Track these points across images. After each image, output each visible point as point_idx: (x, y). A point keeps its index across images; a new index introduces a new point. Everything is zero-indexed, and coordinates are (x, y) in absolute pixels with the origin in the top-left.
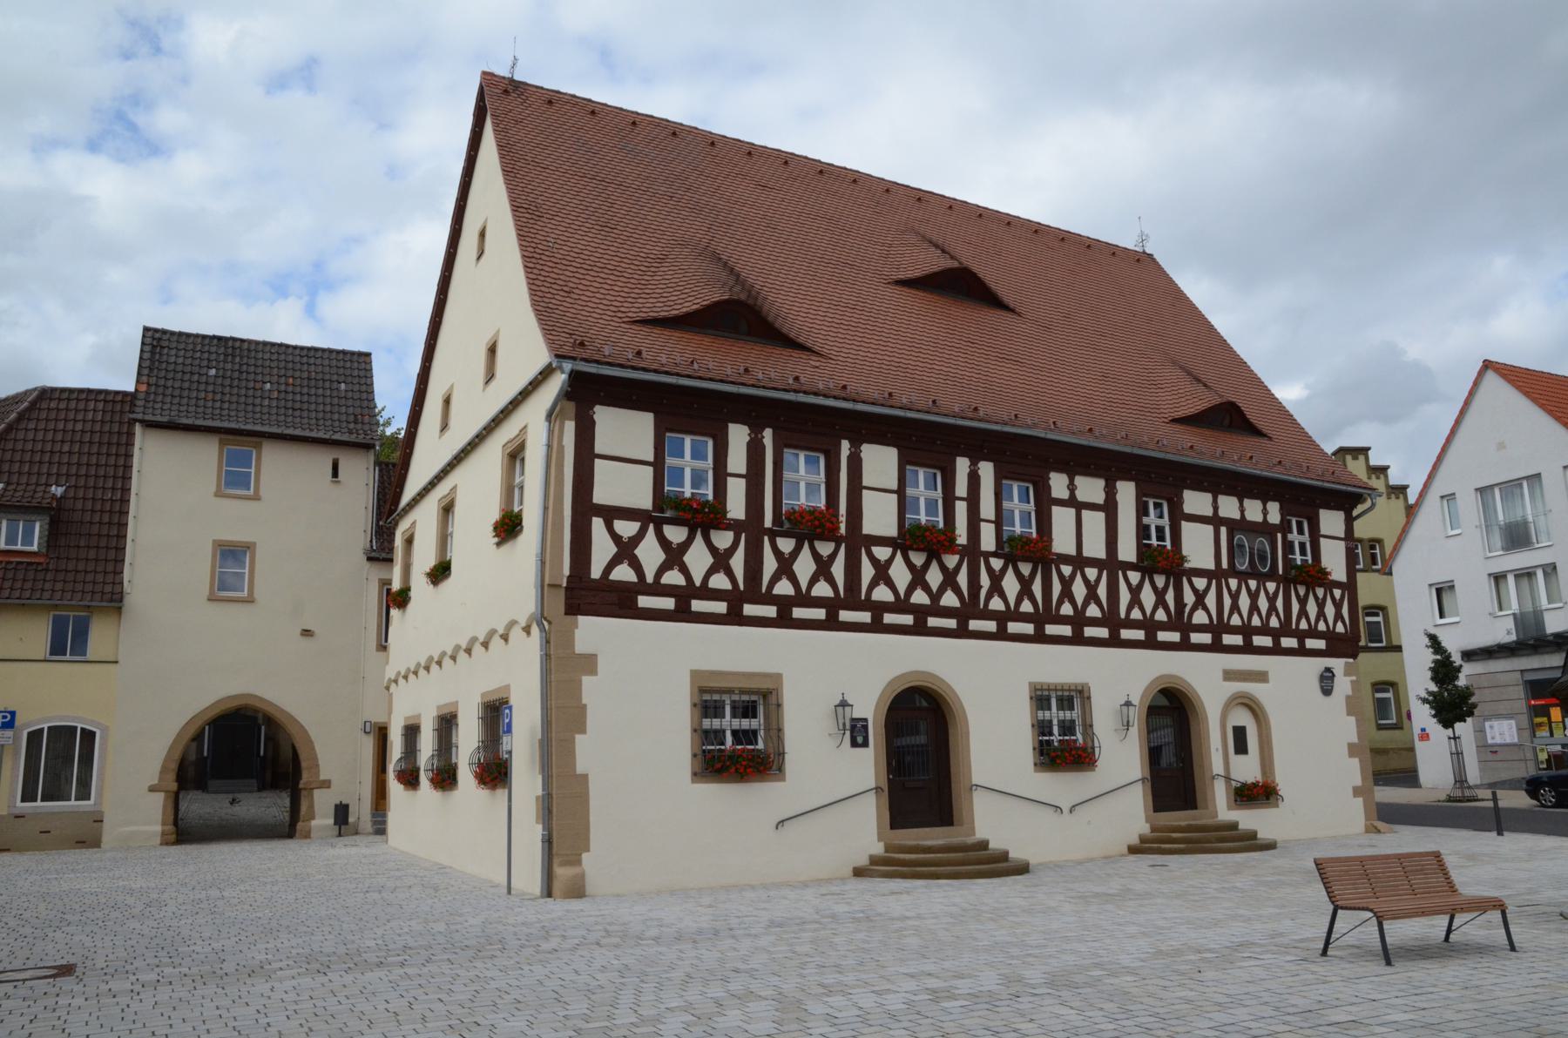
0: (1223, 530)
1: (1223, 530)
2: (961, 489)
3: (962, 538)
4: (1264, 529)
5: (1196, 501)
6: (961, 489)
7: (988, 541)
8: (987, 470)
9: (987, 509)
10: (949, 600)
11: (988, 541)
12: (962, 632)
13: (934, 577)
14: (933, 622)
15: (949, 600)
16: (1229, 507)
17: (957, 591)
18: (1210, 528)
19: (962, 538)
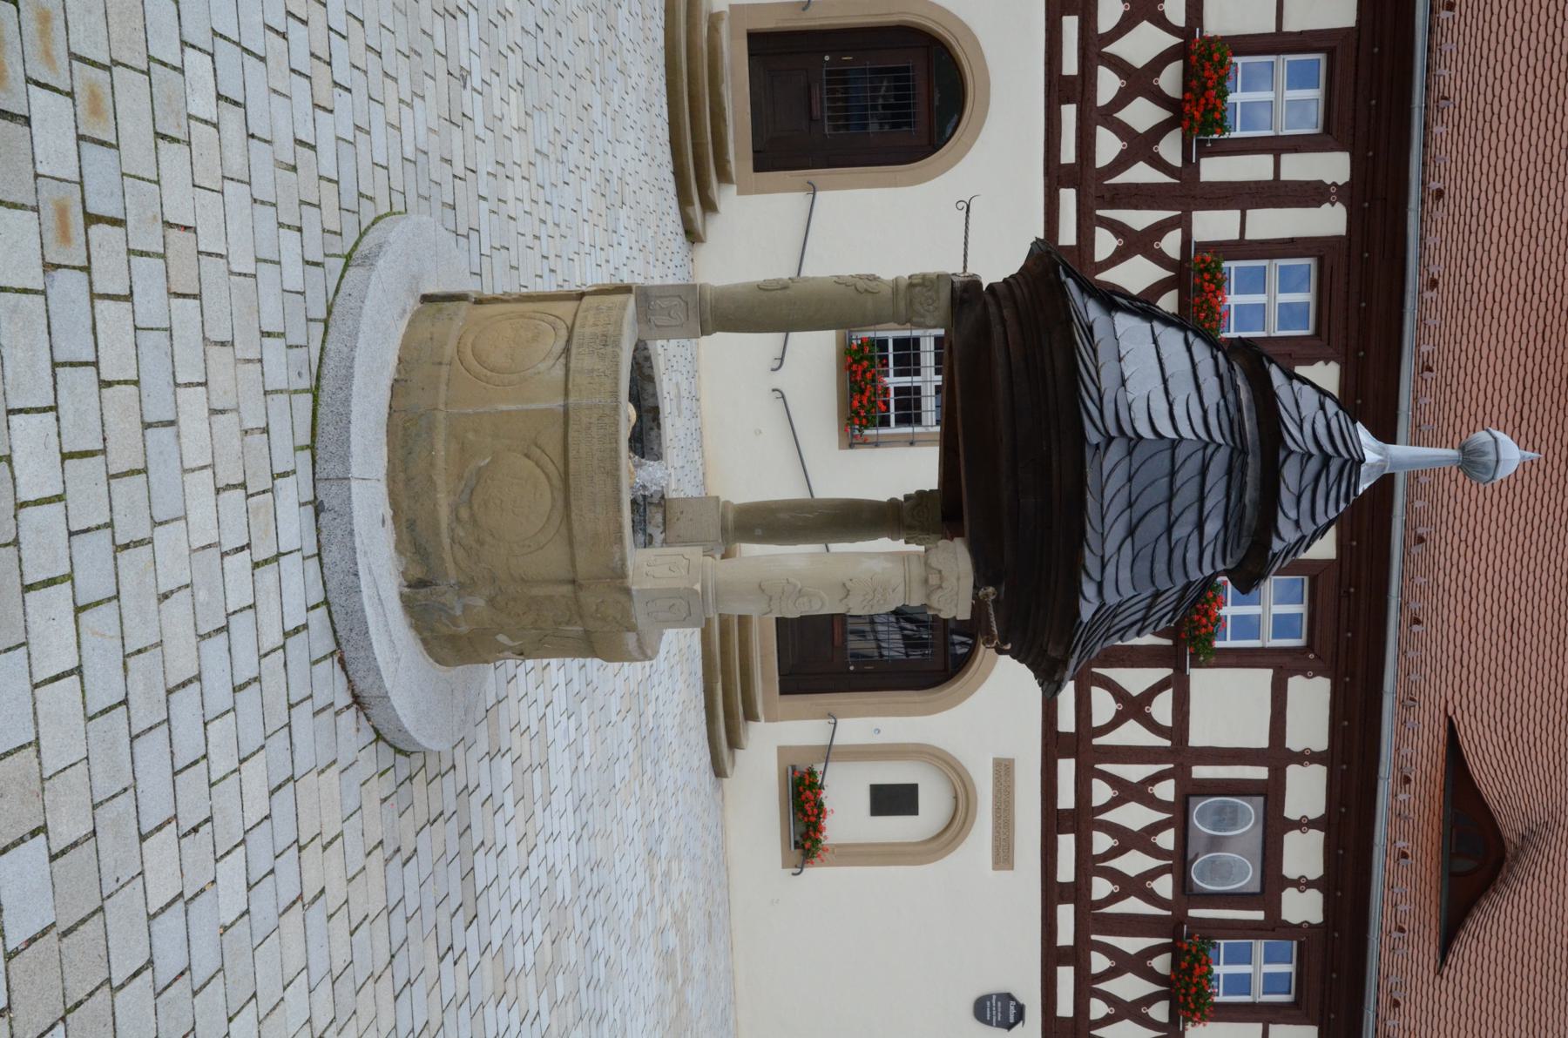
0: (1261, 773)
1: (1261, 773)
2: (1297, 167)
3: (1214, 170)
4: (1273, 881)
5: (1311, 700)
6: (1297, 167)
7: (1214, 225)
8: (1330, 221)
9: (1268, 223)
10: (1108, 146)
11: (1214, 225)
12: (1056, 176)
13: (1142, 114)
14: (1069, 113)
15: (1108, 146)
16: (1306, 791)
17: (1122, 163)
18: (1263, 742)
19: (1214, 170)
